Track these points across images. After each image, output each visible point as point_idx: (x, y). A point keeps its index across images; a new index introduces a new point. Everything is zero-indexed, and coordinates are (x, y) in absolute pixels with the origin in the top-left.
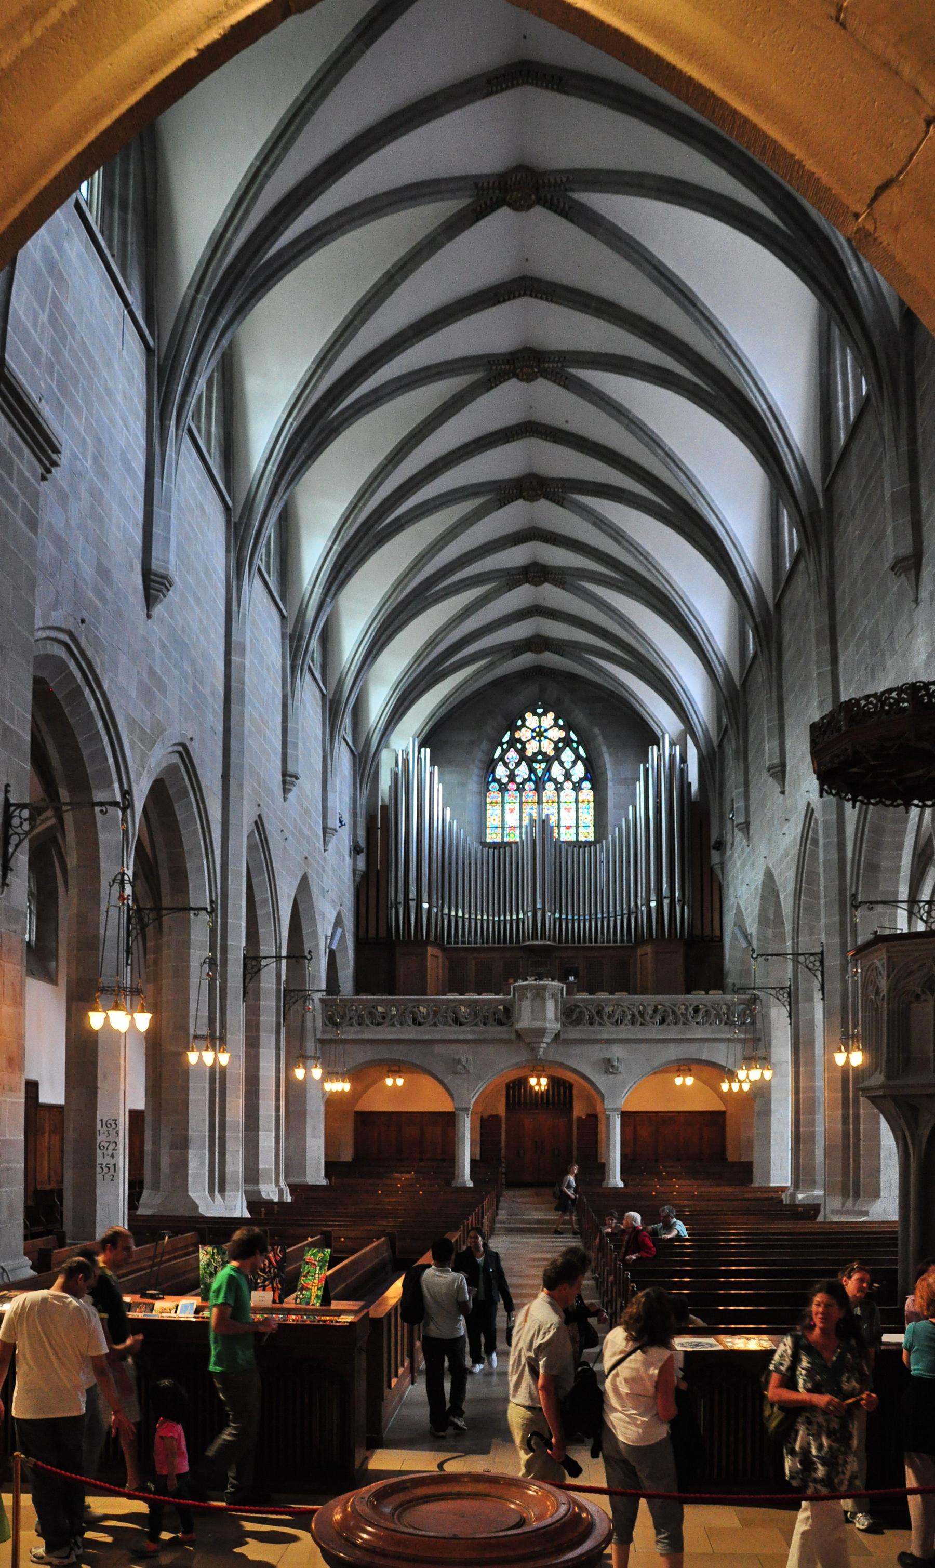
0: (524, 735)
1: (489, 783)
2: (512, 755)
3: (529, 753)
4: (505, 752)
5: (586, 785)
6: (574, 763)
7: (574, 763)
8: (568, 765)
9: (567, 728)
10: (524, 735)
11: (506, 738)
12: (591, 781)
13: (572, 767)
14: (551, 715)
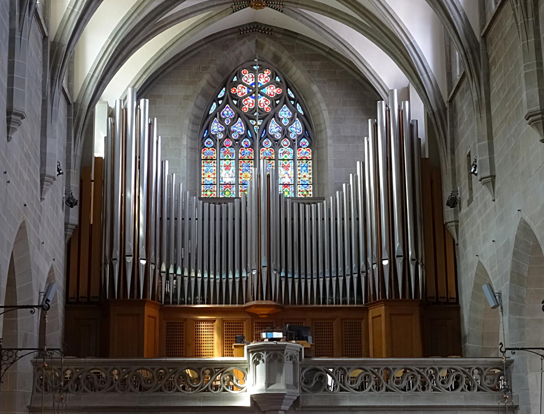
0: (241, 91)
1: (203, 139)
2: (228, 112)
3: (246, 108)
4: (220, 108)
5: (305, 141)
6: (292, 120)
7: (292, 120)
8: (285, 122)
9: (287, 84)
10: (241, 91)
11: (222, 94)
12: (309, 138)
13: (290, 125)
14: (267, 73)
